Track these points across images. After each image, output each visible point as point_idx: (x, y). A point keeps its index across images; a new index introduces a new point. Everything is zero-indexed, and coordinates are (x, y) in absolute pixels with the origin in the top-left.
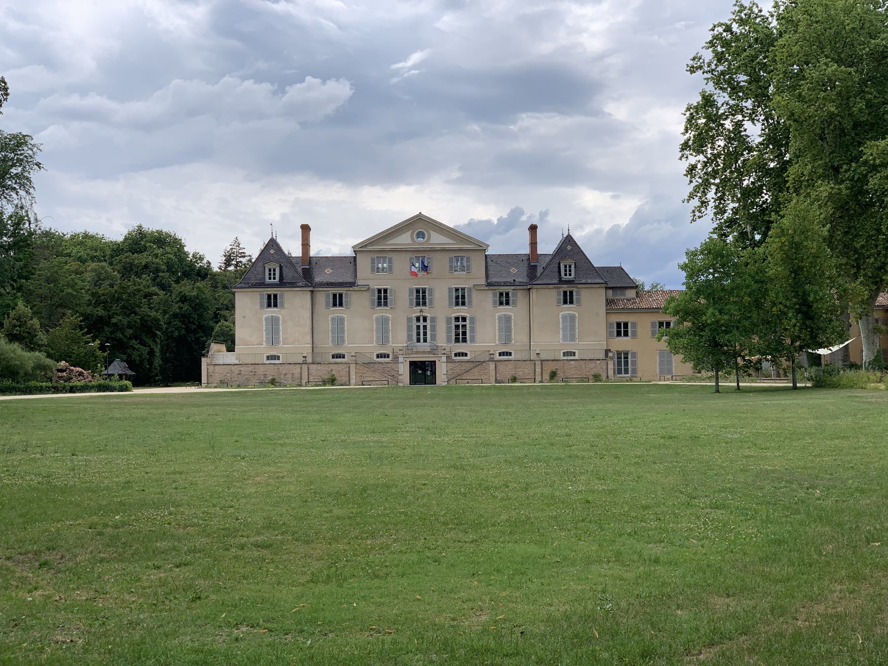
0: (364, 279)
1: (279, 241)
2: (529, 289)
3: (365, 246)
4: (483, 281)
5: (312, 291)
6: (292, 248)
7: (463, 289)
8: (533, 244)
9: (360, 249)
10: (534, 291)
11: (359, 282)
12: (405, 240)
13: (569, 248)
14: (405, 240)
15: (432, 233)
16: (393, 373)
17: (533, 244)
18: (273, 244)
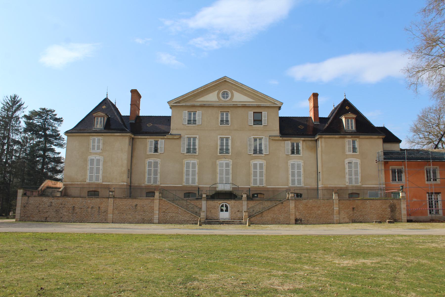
0: (177, 129)
1: (109, 98)
2: (316, 141)
3: (179, 102)
4: (277, 133)
5: (133, 139)
6: (125, 110)
7: (260, 139)
8: (316, 108)
9: (175, 104)
10: (323, 140)
11: (172, 132)
12: (212, 97)
13: (347, 108)
14: (212, 97)
15: (235, 93)
16: (197, 210)
17: (316, 108)
18: (106, 102)
